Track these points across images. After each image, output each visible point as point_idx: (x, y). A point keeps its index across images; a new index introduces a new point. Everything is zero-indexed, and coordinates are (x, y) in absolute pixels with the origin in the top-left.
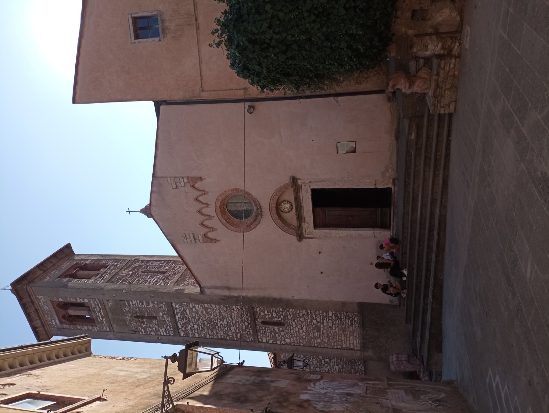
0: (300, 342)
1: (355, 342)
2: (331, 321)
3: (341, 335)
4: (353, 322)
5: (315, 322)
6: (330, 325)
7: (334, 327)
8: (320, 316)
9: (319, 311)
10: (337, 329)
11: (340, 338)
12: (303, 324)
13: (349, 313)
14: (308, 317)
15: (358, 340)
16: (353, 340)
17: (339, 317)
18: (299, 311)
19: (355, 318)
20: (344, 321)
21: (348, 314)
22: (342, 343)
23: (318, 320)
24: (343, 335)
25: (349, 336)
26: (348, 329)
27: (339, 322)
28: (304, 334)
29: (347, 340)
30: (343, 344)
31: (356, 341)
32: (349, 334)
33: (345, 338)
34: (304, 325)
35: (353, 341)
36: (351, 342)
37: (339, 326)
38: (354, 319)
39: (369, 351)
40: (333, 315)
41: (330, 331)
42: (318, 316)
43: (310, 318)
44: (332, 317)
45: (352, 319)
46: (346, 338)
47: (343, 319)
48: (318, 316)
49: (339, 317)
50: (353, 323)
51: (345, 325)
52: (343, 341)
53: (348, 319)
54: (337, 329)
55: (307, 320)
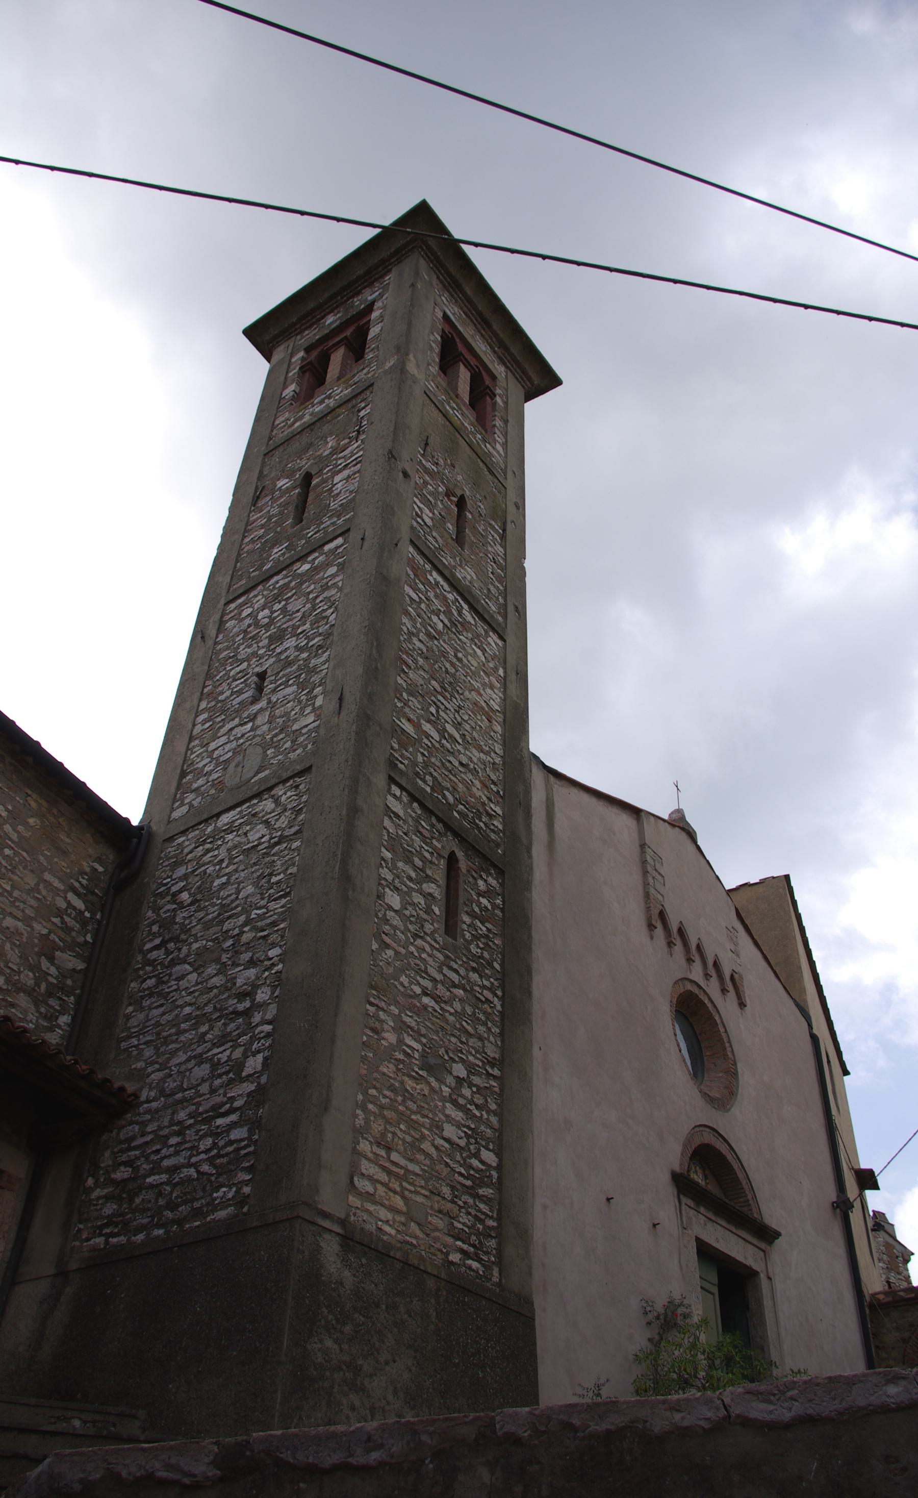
0: (388, 946)
1: (384, 1214)
2: (462, 1143)
3: (411, 1160)
4: (465, 1247)
5: (459, 1070)
6: (450, 1131)
7: (442, 1142)
8: (478, 1107)
9: (495, 1113)
10: (434, 1153)
11: (401, 1148)
12: (451, 1014)
13: (493, 1243)
14: (474, 1052)
15: (393, 1232)
16: (393, 1209)
17: (481, 1192)
18: (493, 1031)
19: (479, 1260)
20: (465, 1203)
21: (492, 1237)
22: (379, 1144)
23: (467, 1092)
24: (412, 1167)
25: (406, 1193)
26: (436, 1206)
27: (461, 1179)
28: (418, 990)
29: (389, 1173)
30: (371, 1143)
31: (387, 1222)
32: (413, 1196)
33: (402, 1172)
34: (447, 1014)
35: (383, 1205)
36: (381, 1190)
37: (446, 1171)
38: (476, 1254)
39: (347, 1273)
40: (484, 1168)
41: (426, 1112)
42: (479, 1100)
43: (471, 1058)
44: (477, 1155)
45: (474, 1246)
46: (397, 1177)
47: (471, 1201)
48: (479, 1100)
49: (481, 1192)
50: (459, 1243)
51: (453, 1202)
52: (383, 1153)
53: (473, 1226)
54: (434, 1153)
55: (464, 1040)
